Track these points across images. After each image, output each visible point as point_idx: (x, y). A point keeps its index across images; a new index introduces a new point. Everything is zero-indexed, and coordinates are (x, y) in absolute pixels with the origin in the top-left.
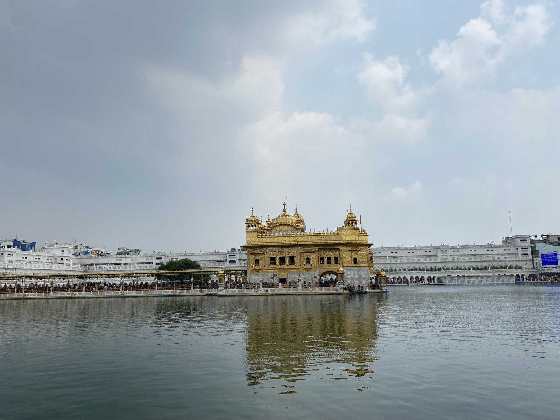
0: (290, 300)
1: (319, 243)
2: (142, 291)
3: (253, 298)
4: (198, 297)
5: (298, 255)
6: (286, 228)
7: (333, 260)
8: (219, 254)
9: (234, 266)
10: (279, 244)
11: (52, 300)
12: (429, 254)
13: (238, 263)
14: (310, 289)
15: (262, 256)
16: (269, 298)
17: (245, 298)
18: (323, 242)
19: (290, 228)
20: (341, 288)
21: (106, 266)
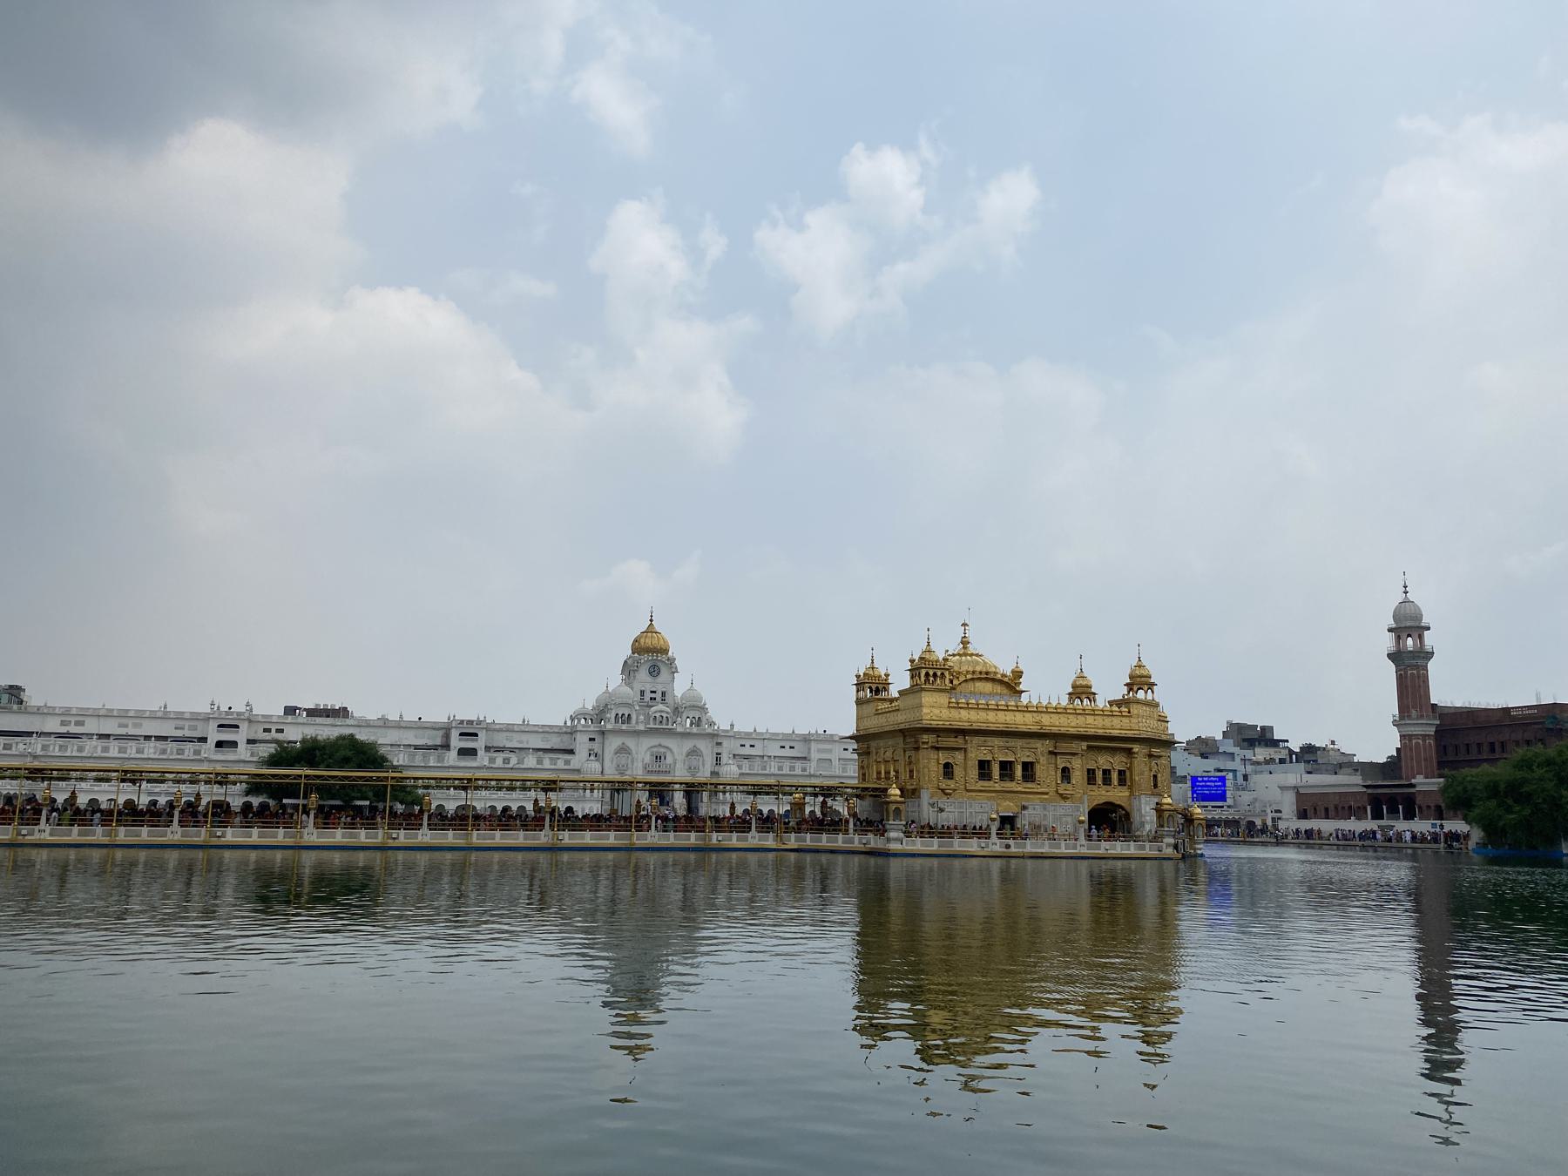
0: (931, 870)
1: (1091, 732)
2: (612, 834)
3: (975, 861)
4: (771, 855)
5: (1043, 760)
6: (988, 687)
7: (1115, 776)
8: (419, 726)
9: (474, 764)
10: (1001, 727)
11: (313, 855)
13: (483, 758)
15: (959, 756)
16: (1013, 861)
17: (957, 863)
18: (1100, 732)
19: (999, 689)
20: (1168, 845)
21: (33, 739)
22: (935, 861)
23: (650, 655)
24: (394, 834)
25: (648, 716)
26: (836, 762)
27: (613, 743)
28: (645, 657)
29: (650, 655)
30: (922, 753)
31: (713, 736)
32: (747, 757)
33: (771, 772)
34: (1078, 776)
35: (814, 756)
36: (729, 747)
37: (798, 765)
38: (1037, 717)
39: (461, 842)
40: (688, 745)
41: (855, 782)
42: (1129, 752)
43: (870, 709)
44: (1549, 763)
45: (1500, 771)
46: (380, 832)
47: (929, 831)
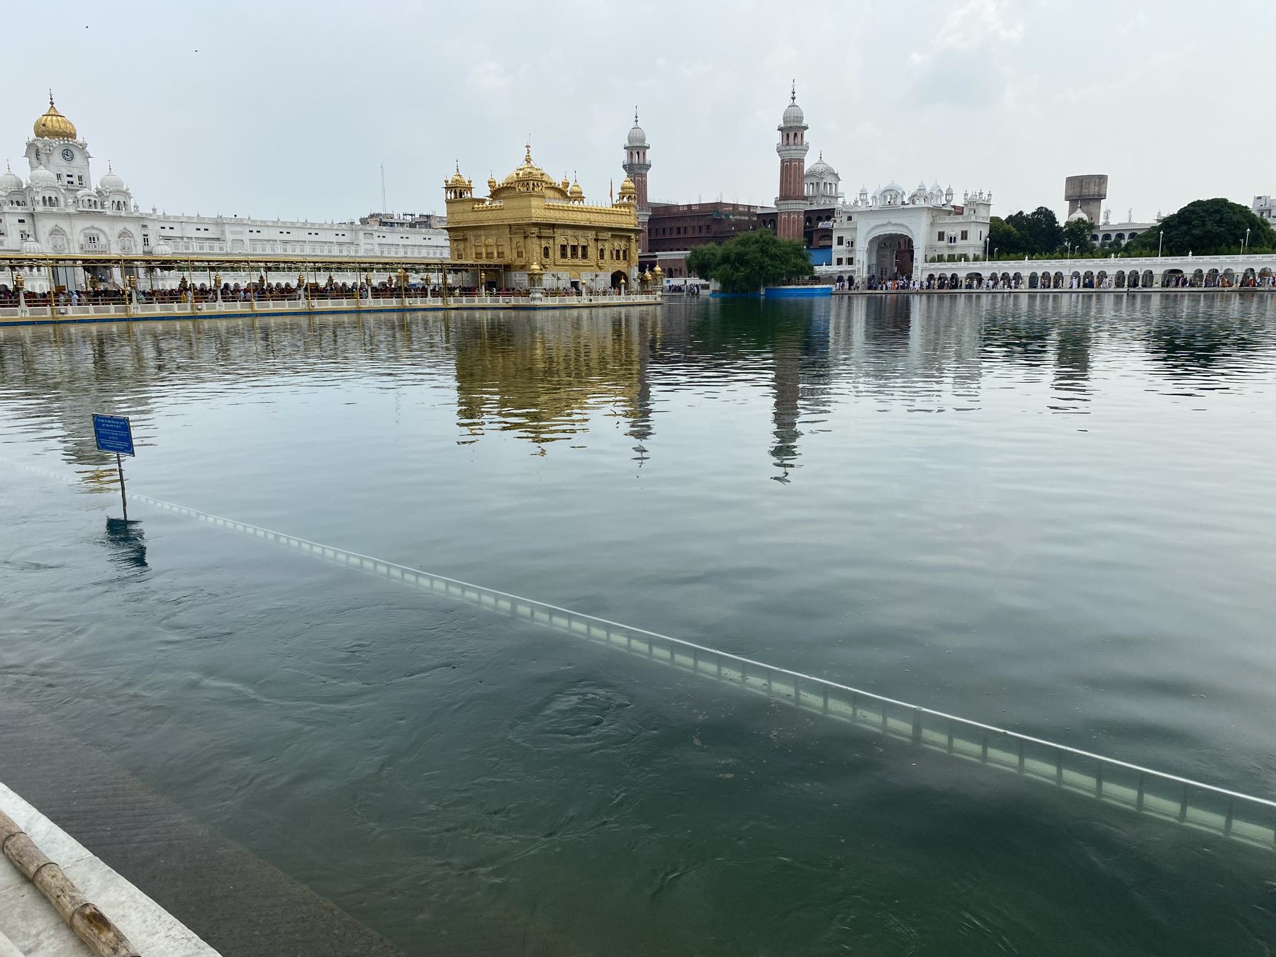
3: (575, 312)
5: (592, 244)
12: (342, 239)
14: (632, 297)
15: (551, 241)
17: (567, 312)
19: (557, 195)
22: (557, 312)
23: (54, 138)
24: (199, 305)
25: (76, 202)
26: (247, 242)
27: (45, 226)
28: (56, 142)
29: (54, 138)
30: (529, 240)
31: (141, 218)
32: (168, 239)
33: (195, 250)
34: (607, 254)
35: (229, 236)
36: (153, 230)
37: (216, 244)
38: (588, 215)
39: (247, 310)
40: (119, 227)
41: (450, 261)
42: (629, 238)
43: (458, 207)
44: (757, 242)
45: (730, 246)
46: (189, 305)
47: (553, 293)
